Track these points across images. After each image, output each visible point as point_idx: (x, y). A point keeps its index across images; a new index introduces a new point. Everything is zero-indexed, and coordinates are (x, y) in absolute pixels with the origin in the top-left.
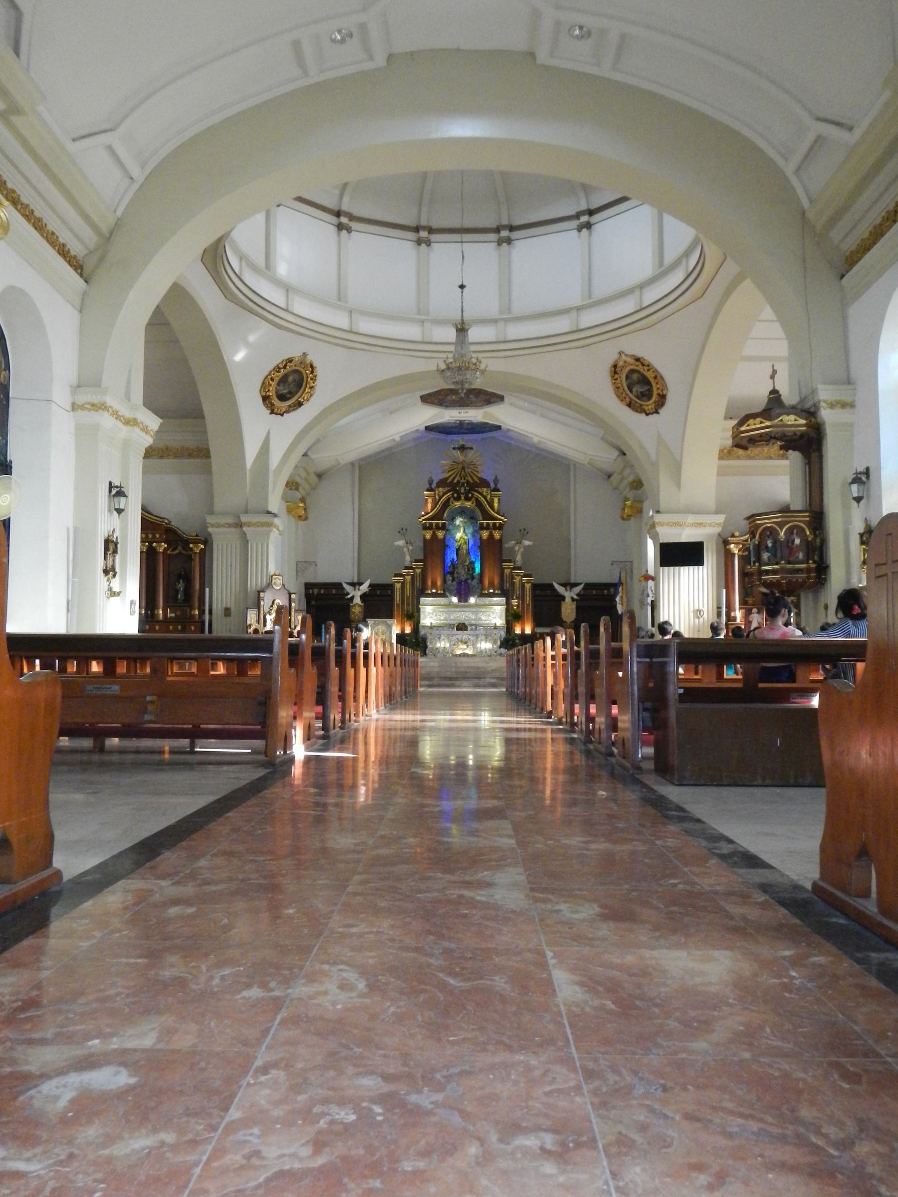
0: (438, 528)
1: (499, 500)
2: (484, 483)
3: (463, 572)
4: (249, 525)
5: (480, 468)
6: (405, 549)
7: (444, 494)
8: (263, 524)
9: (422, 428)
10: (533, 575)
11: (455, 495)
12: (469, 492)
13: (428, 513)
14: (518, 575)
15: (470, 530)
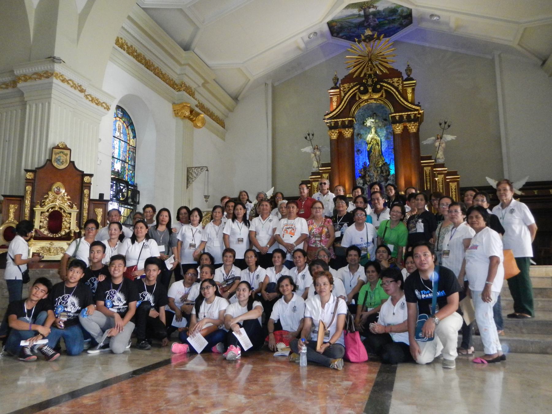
0: (344, 126)
1: (413, 90)
2: (395, 73)
3: (375, 174)
4: (26, 78)
5: (389, 59)
6: (313, 155)
7: (349, 91)
8: (39, 76)
9: (326, 28)
10: (458, 174)
11: (362, 88)
12: (377, 83)
13: (334, 111)
14: (440, 173)
15: (383, 133)
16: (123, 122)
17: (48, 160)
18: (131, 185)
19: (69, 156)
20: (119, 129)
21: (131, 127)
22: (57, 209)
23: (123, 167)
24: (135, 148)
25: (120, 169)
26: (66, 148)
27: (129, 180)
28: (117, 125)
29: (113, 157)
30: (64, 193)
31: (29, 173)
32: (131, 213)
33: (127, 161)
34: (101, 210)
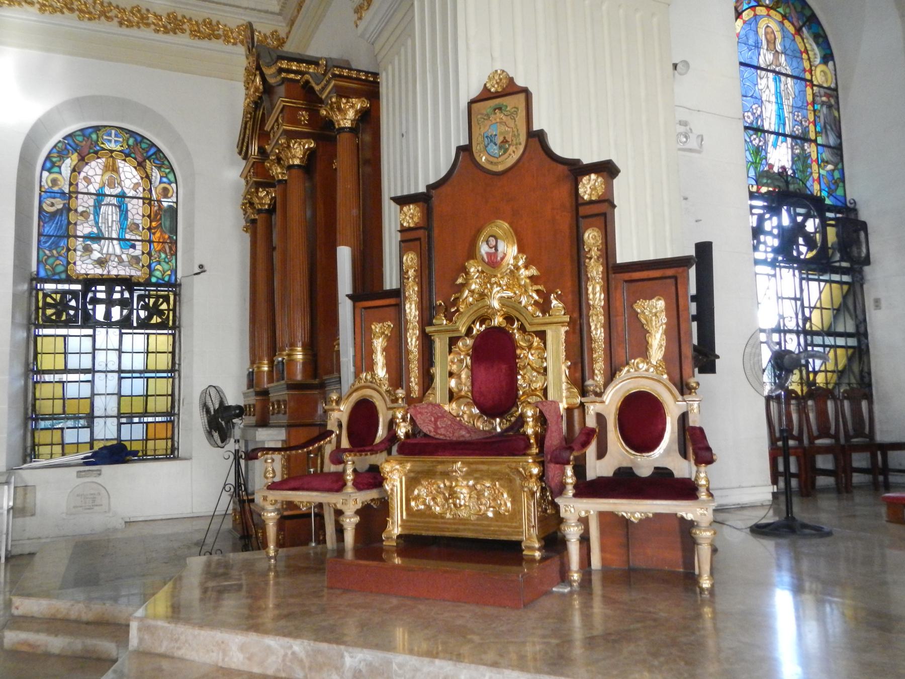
16: (779, 18)
17: (460, 149)
18: (830, 209)
19: (522, 113)
20: (771, 43)
21: (809, 29)
22: (498, 321)
23: (798, 156)
24: (833, 92)
25: (788, 165)
26: (511, 89)
27: (824, 194)
28: (762, 31)
29: (756, 129)
30: (515, 258)
31: (405, 209)
32: (845, 297)
33: (812, 136)
34: (661, 304)
